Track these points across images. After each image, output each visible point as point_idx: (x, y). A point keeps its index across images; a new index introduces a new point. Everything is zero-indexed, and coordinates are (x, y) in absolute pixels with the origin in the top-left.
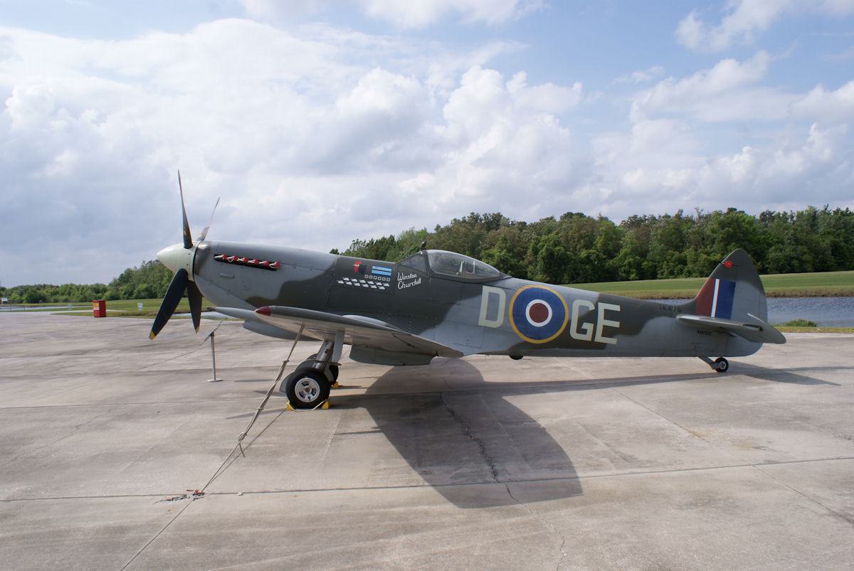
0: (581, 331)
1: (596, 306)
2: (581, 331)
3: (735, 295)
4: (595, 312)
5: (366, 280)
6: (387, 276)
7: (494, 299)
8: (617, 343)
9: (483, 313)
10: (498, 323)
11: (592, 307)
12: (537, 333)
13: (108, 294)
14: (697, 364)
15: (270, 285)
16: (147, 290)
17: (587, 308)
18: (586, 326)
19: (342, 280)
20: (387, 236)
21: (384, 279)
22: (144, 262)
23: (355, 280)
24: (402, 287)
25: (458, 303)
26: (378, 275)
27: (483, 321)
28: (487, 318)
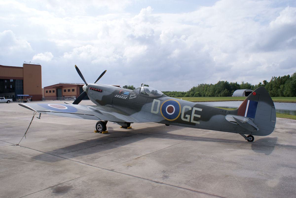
0: (185, 117)
1: (192, 109)
2: (185, 117)
3: (257, 107)
4: (192, 111)
6: (127, 95)
7: (156, 104)
8: (200, 123)
10: (157, 112)
11: (190, 109)
12: (170, 117)
13: (186, 95)
14: (238, 137)
16: (198, 94)
17: (189, 109)
18: (187, 116)
19: (116, 95)
20: (287, 75)
21: (126, 96)
22: (199, 84)
23: (119, 96)
25: (145, 104)
26: (125, 94)
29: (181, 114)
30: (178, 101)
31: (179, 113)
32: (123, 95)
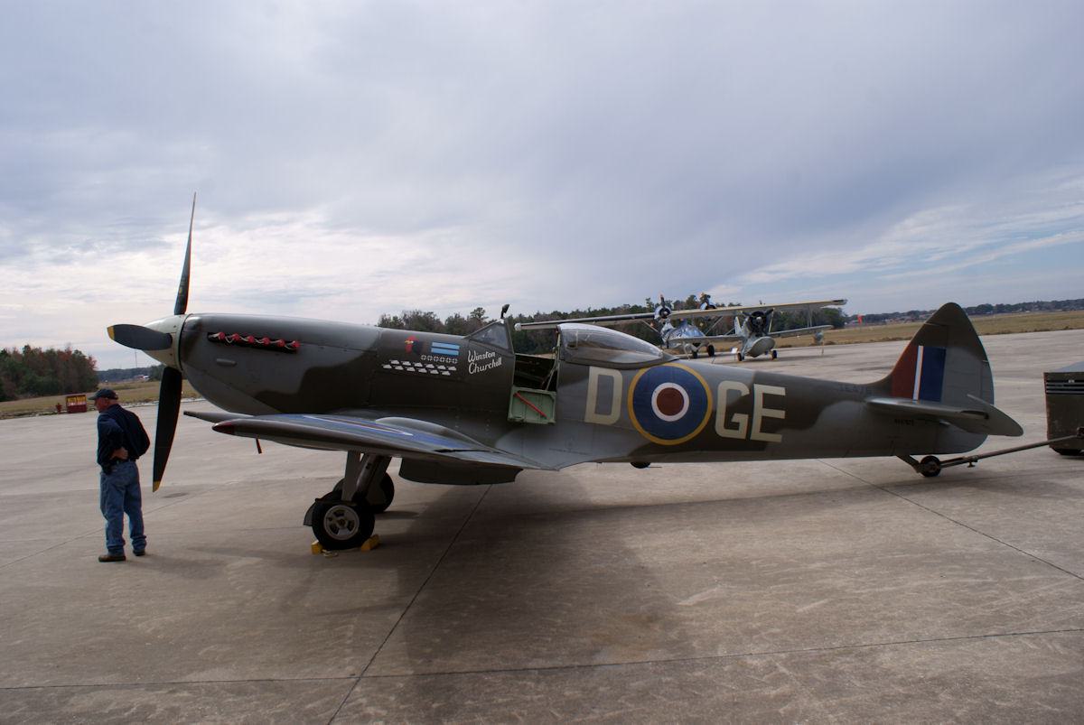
0: (730, 425)
2: (730, 425)
4: (750, 398)
5: (423, 362)
6: (452, 357)
7: (605, 384)
8: (783, 440)
9: (591, 404)
11: (745, 391)
14: (891, 465)
15: (288, 375)
18: (737, 418)
21: (449, 360)
23: (407, 363)
24: (475, 371)
26: (440, 355)
27: (591, 416)
28: (598, 411)
29: (714, 414)
30: (691, 368)
31: (706, 411)
32: (430, 358)
